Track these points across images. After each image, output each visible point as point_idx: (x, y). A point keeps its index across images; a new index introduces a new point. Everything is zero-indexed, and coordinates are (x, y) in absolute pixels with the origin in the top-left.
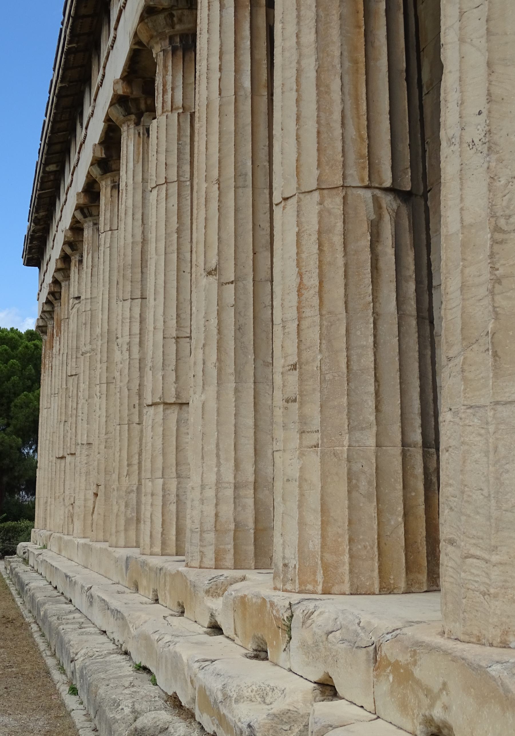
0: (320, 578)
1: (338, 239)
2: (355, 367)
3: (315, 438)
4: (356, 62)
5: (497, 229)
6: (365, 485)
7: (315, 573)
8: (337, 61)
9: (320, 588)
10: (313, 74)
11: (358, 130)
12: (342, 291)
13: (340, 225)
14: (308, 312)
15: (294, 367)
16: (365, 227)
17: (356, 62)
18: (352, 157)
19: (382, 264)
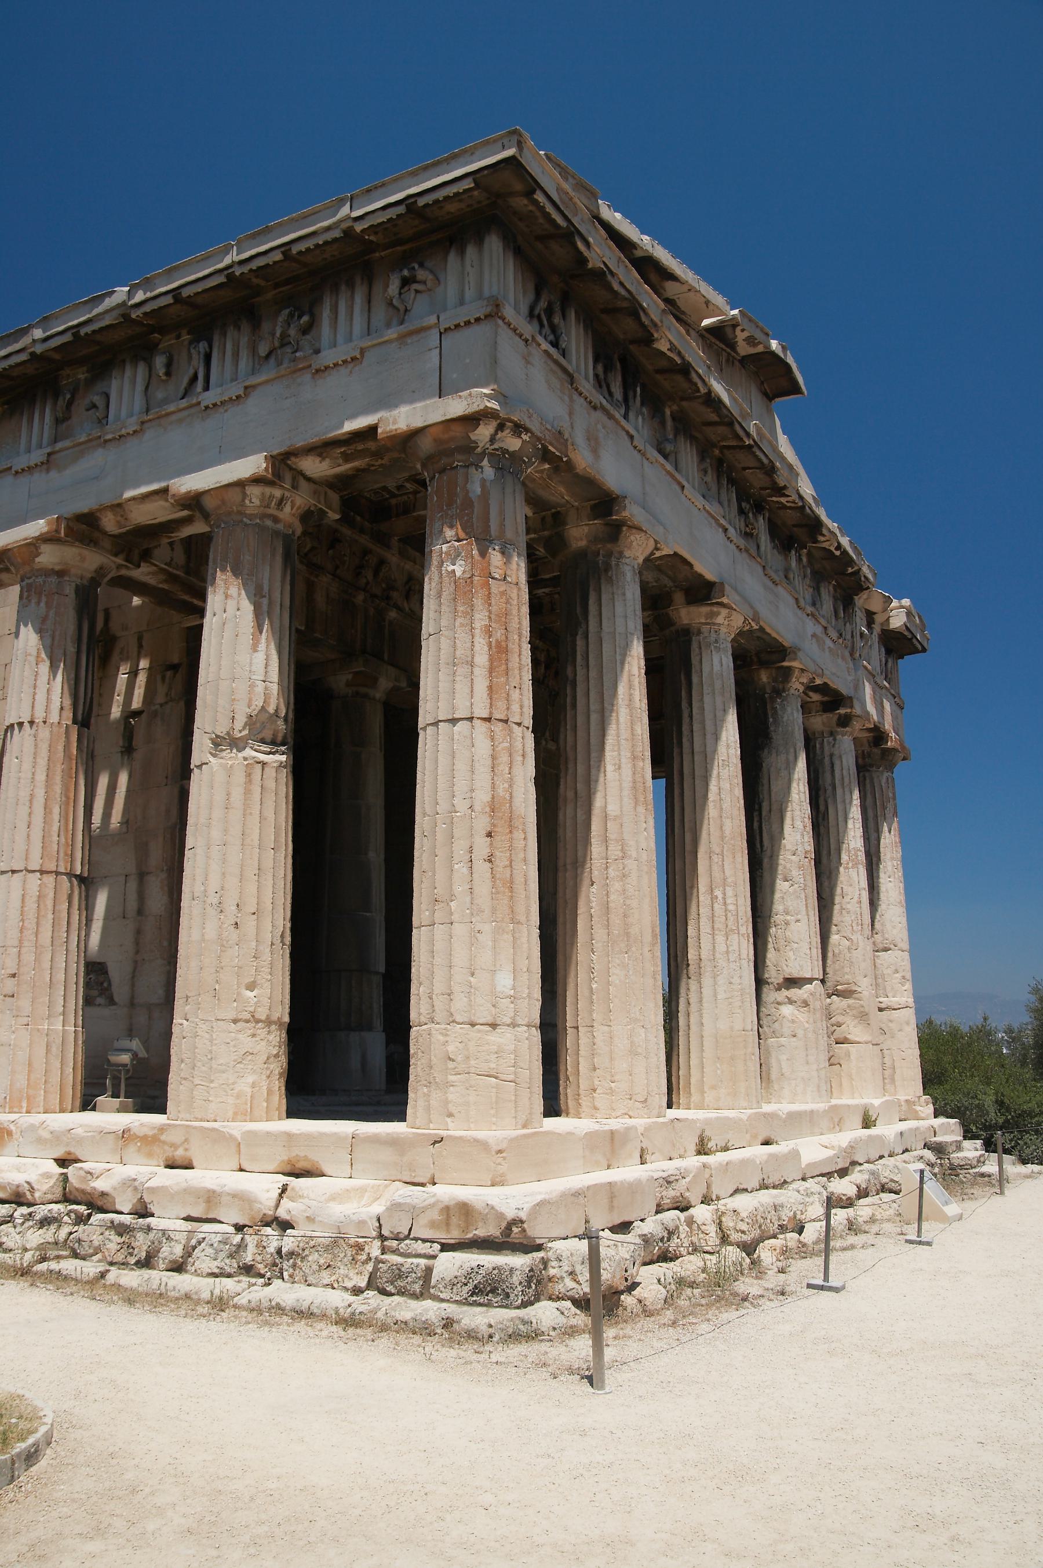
0: (24, 1105)
1: (50, 903)
2: (53, 980)
3: (25, 1020)
4: (68, 798)
5: (223, 946)
6: (55, 1050)
7: (20, 1101)
8: (58, 796)
9: (24, 1110)
10: (42, 801)
11: (66, 839)
12: (50, 934)
13: (51, 895)
14: (26, 944)
15: (14, 976)
16: (66, 897)
17: (68, 798)
18: (62, 854)
19: (71, 920)
